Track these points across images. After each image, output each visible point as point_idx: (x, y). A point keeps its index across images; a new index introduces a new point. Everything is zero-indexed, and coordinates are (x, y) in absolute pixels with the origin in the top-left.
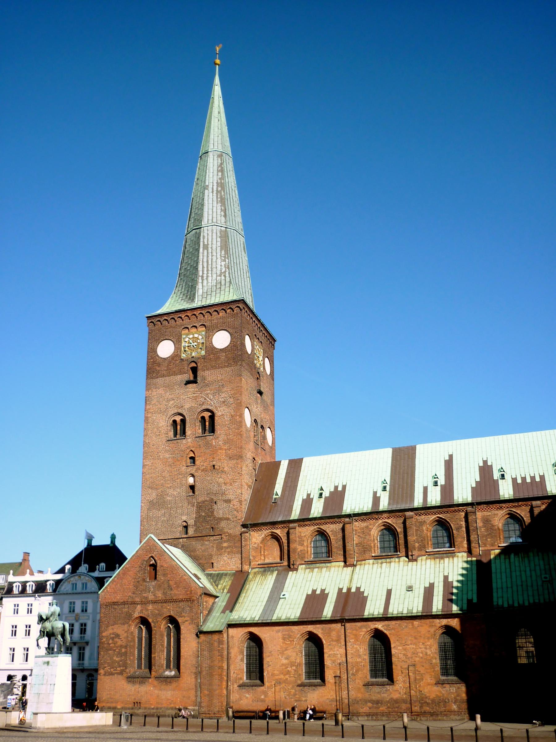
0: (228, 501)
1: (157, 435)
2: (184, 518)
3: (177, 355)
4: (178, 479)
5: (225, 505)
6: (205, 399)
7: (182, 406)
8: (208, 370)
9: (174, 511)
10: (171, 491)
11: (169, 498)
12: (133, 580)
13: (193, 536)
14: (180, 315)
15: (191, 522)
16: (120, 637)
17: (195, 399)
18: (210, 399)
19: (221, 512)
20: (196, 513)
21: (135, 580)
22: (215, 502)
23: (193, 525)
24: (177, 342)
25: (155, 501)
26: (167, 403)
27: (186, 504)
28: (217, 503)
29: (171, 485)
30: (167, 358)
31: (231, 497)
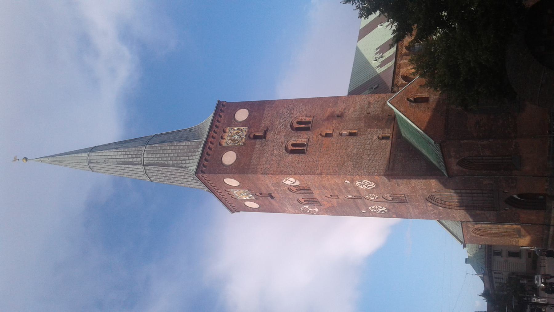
0: (369, 104)
1: (298, 163)
2: (375, 137)
3: (238, 149)
4: (341, 144)
5: (372, 106)
6: (283, 125)
7: (282, 142)
8: (260, 124)
9: (367, 146)
10: (349, 149)
11: (355, 152)
12: (426, 113)
13: (392, 130)
14: (208, 147)
15: (380, 133)
16: (480, 120)
17: (280, 132)
18: (284, 121)
19: (376, 109)
20: (373, 128)
21: (426, 111)
22: (368, 114)
23: (383, 130)
24: (228, 148)
25: (354, 163)
26: (274, 155)
27: (364, 136)
28: (369, 113)
29: (344, 149)
30: (237, 156)
31: (367, 102)
